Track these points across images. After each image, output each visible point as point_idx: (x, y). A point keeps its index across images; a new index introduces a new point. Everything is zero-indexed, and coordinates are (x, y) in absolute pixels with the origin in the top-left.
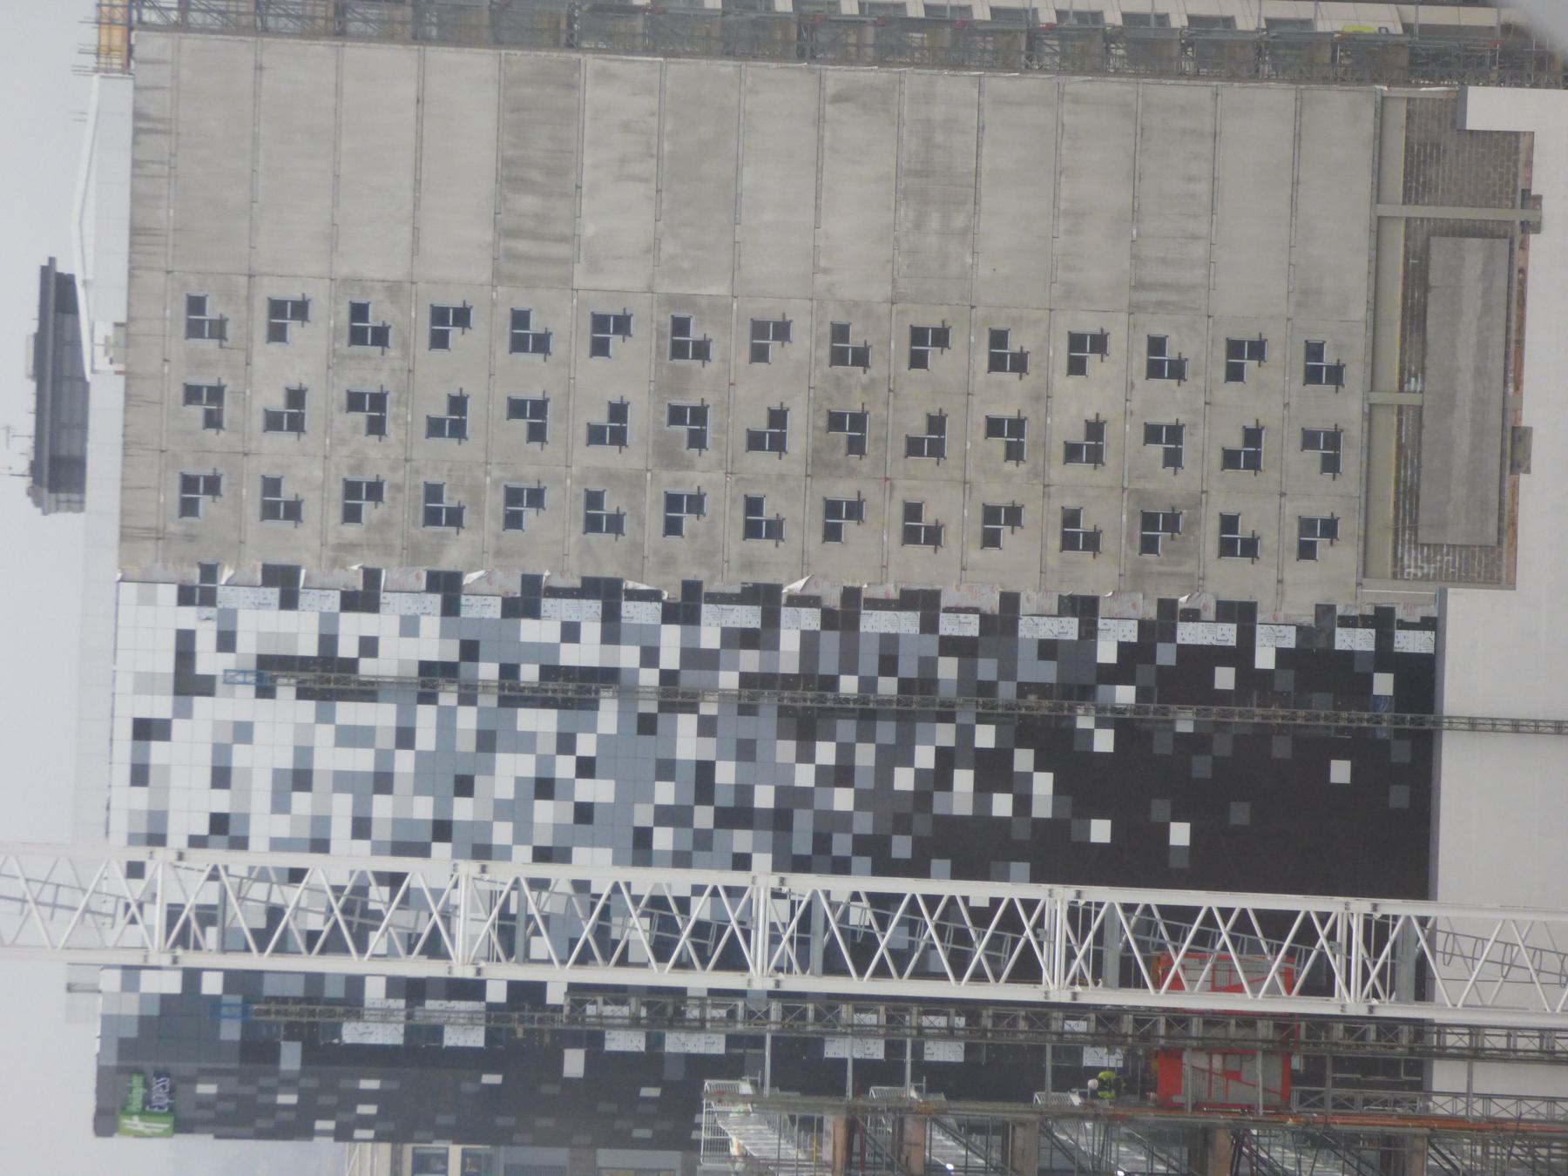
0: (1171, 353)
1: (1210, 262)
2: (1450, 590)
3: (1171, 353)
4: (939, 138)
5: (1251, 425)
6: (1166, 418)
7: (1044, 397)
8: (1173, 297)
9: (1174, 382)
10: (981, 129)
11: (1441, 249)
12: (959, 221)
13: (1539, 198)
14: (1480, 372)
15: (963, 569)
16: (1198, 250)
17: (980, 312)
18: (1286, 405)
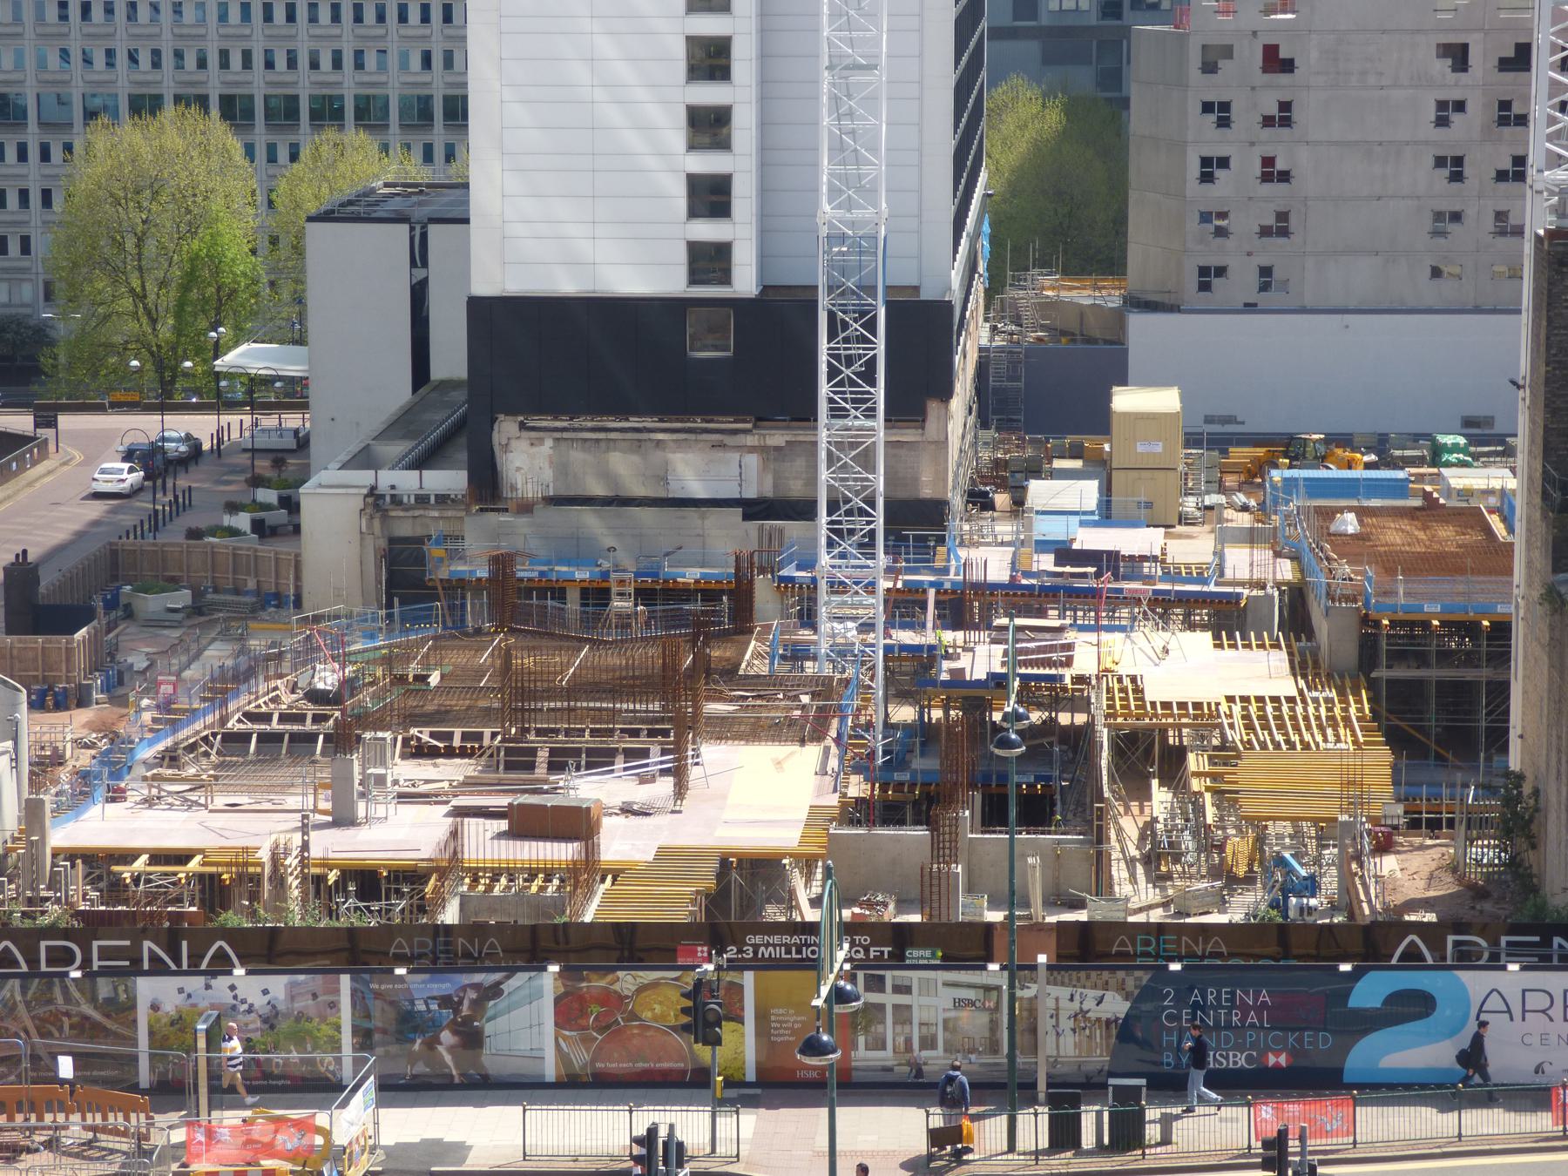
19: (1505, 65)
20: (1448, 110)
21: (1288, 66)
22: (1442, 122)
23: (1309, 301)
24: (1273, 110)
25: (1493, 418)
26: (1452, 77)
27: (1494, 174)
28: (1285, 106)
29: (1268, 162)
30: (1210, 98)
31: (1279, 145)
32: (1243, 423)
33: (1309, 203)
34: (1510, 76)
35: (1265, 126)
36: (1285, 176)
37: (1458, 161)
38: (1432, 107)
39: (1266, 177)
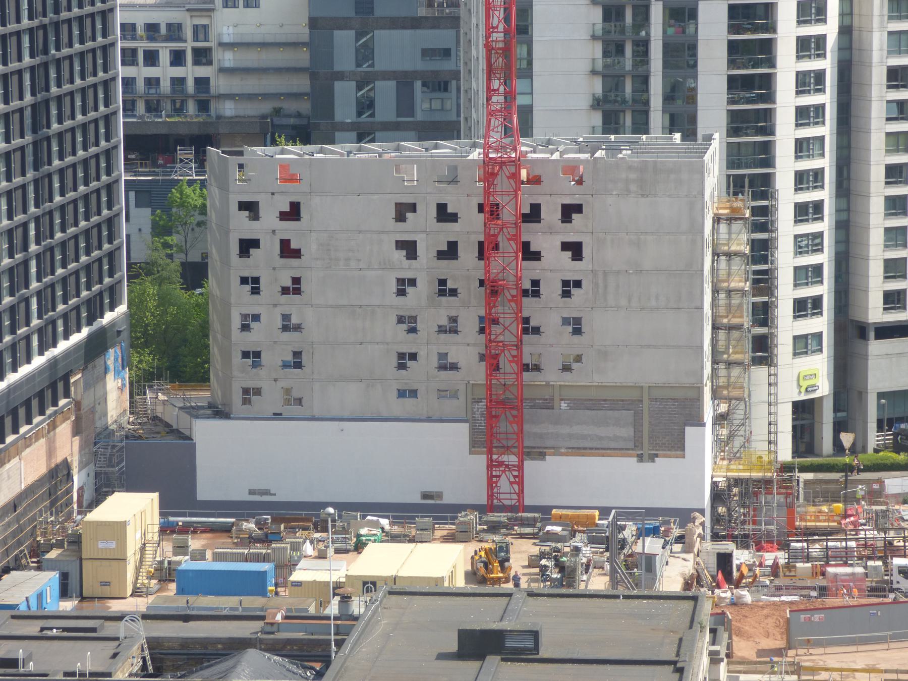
0: (574, 291)
1: (618, 308)
2: (467, 425)
3: (574, 291)
4: (672, 176)
5: (542, 330)
6: (543, 289)
7: (551, 231)
8: (601, 291)
9: (560, 292)
10: (678, 196)
11: (628, 415)
12: (633, 187)
13: (653, 461)
14: (571, 436)
15: (468, 195)
16: (623, 302)
17: (590, 199)
18: (552, 346)
19: (441, 255)
20: (404, 286)
21: (297, 254)
22: (401, 293)
23: (317, 413)
24: (288, 283)
25: (442, 493)
26: (406, 263)
27: (436, 329)
28: (296, 281)
29: (286, 317)
30: (246, 274)
31: (292, 305)
32: (275, 495)
33: (314, 346)
34: (445, 263)
35: (283, 294)
36: (298, 328)
37: (413, 319)
38: (394, 283)
39: (285, 328)
